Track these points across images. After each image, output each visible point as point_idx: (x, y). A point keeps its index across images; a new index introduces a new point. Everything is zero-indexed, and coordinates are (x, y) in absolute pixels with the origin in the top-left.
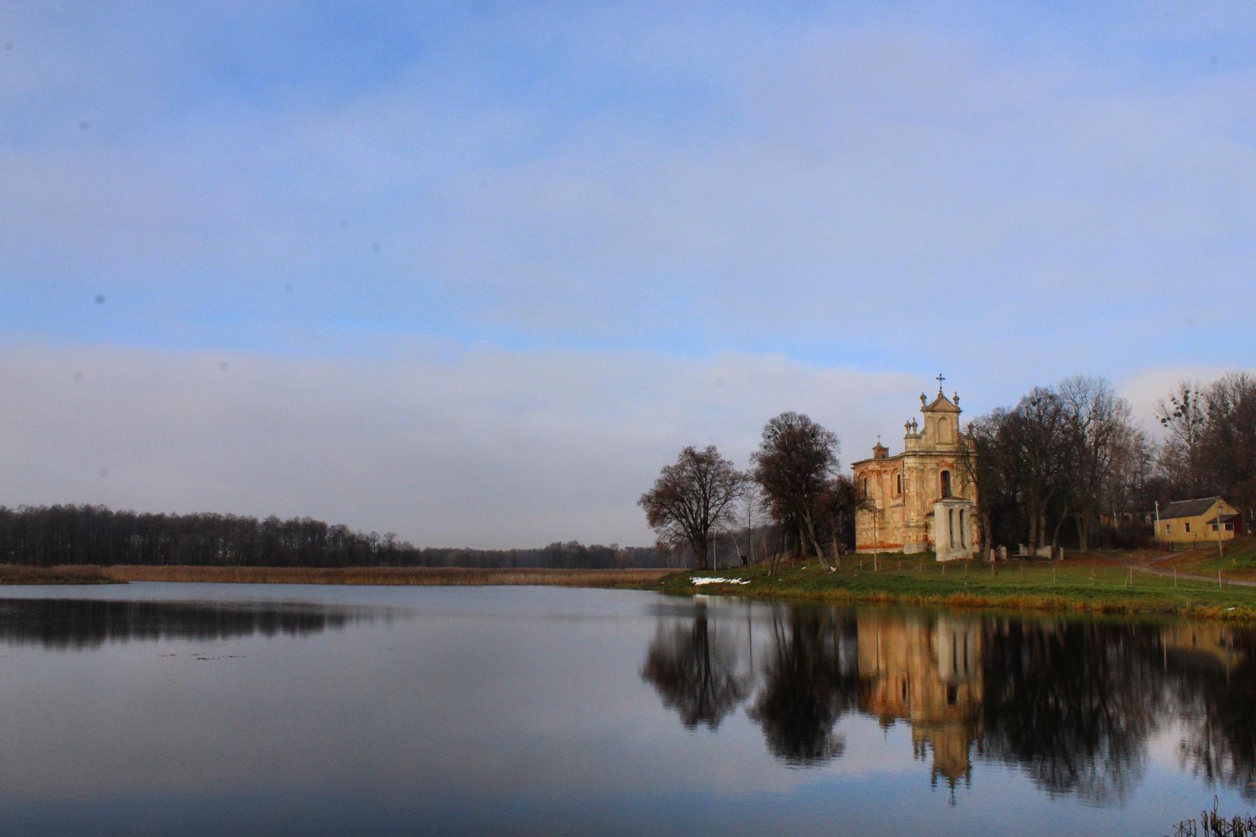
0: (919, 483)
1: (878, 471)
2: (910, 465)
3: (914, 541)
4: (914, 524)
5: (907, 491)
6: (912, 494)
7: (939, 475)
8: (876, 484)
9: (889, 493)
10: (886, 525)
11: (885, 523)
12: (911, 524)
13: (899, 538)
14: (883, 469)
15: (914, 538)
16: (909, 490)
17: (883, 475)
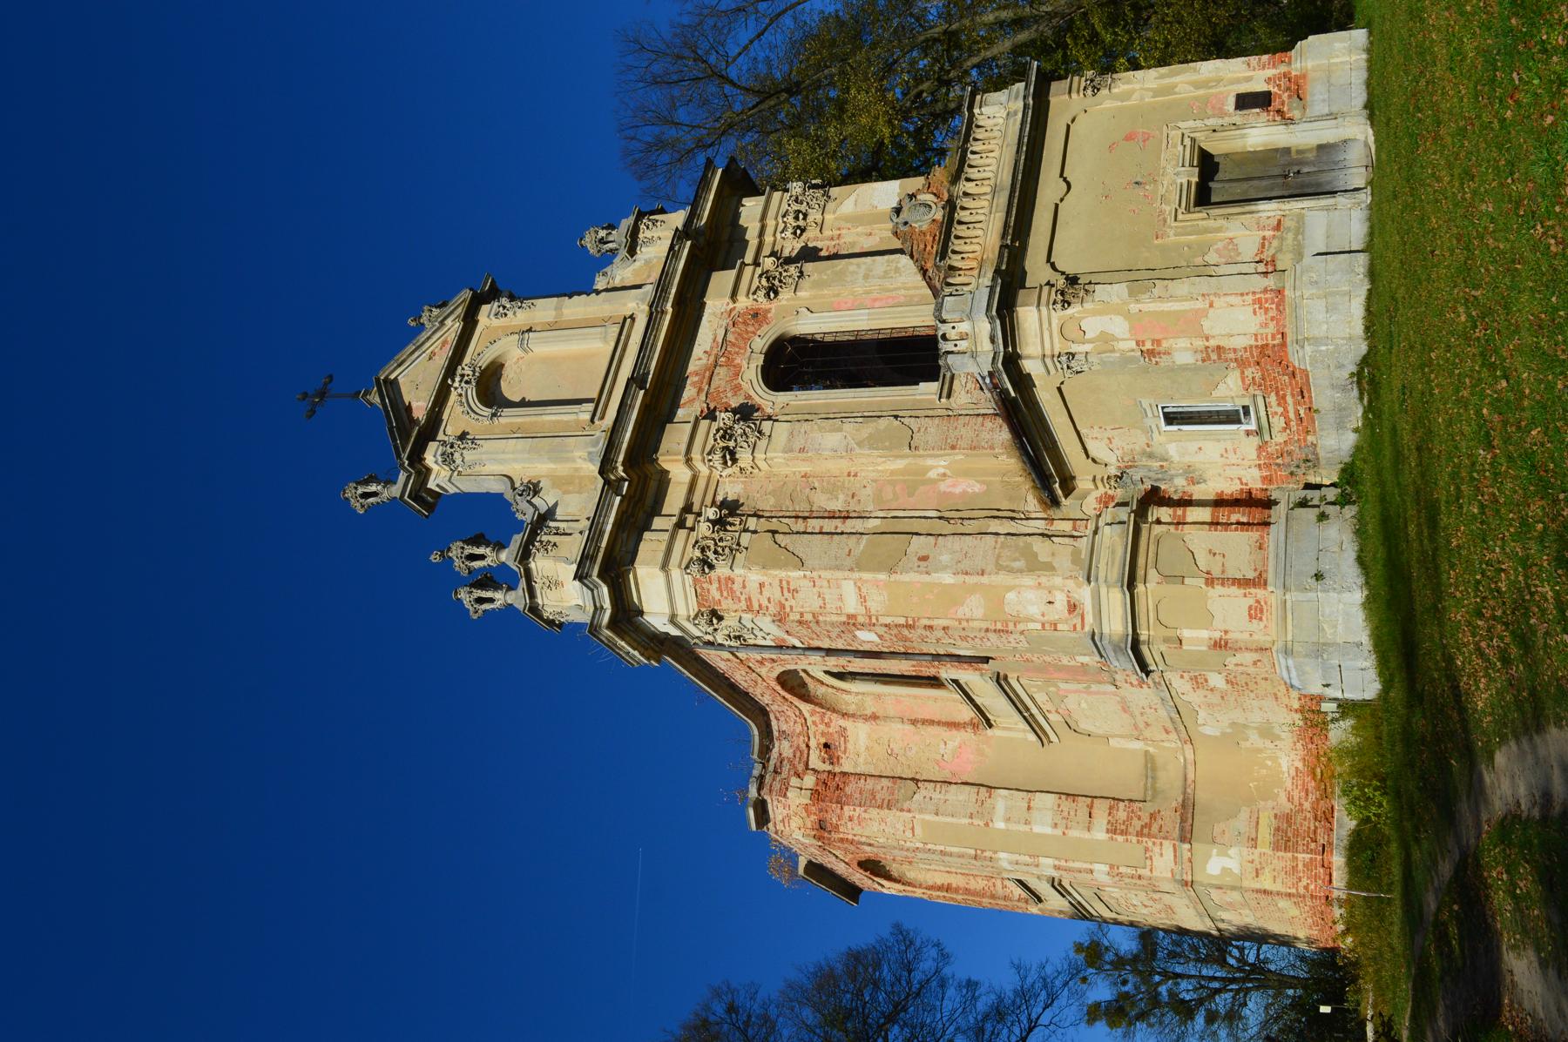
0: (799, 544)
1: (816, 795)
2: (686, 606)
3: (1256, 613)
4: (1115, 600)
5: (867, 638)
6: (877, 602)
7: (783, 398)
8: (891, 816)
9: (957, 738)
10: (1169, 779)
11: (1152, 790)
12: (1115, 624)
13: (1256, 718)
14: (815, 761)
15: (1229, 609)
16: (851, 623)
17: (847, 766)
